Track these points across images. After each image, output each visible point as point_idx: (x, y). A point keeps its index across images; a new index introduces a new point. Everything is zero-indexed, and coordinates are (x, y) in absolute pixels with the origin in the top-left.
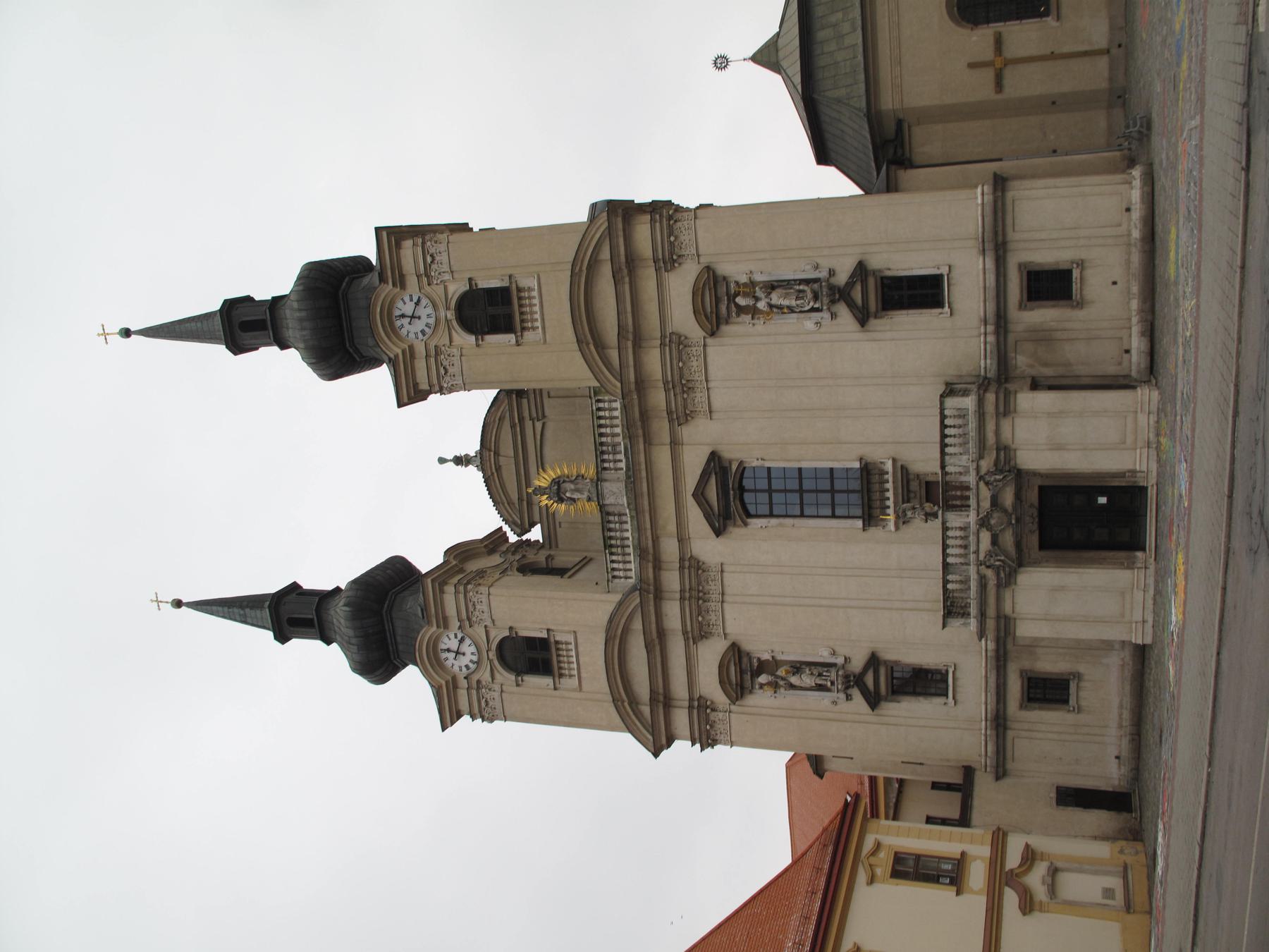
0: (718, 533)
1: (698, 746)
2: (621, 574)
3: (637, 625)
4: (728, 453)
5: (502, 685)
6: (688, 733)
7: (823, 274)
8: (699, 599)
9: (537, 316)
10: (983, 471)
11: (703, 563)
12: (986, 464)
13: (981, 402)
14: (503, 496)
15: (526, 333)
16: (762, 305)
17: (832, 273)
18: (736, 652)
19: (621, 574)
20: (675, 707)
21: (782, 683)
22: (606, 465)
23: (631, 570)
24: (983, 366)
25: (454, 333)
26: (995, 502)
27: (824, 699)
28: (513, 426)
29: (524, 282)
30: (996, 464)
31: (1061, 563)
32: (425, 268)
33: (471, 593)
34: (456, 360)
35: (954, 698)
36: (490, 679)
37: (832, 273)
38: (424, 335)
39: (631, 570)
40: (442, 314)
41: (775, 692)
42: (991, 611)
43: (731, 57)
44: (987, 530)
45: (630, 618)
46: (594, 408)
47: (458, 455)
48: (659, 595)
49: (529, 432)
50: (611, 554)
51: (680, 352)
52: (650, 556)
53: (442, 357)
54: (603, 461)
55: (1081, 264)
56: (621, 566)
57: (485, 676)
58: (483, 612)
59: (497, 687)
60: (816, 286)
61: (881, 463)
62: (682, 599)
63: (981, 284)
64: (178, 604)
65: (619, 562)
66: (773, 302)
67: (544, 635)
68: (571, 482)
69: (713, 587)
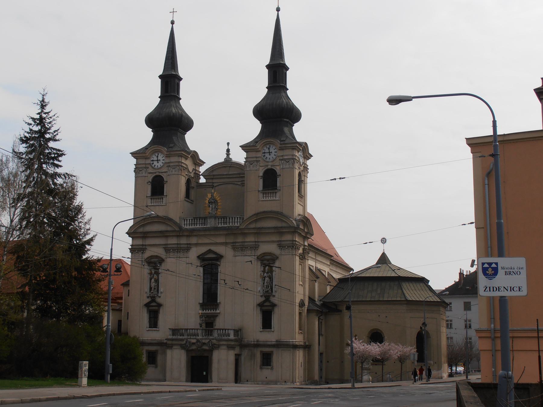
0: (198, 257)
1: (130, 247)
2: (186, 223)
3: (169, 229)
4: (222, 260)
5: (147, 176)
6: (134, 244)
7: (274, 294)
8: (178, 250)
9: (267, 199)
10: (213, 341)
11: (189, 251)
12: (214, 341)
13: (231, 340)
14: (215, 168)
15: (262, 194)
16: (265, 274)
17: (274, 296)
18: (161, 261)
19: (186, 223)
20: (143, 240)
21: (152, 276)
22: (220, 219)
23: (187, 226)
24: (245, 340)
25: (264, 167)
26: (204, 344)
27: (147, 289)
28: (239, 174)
29: (278, 194)
30: (214, 344)
31: (187, 362)
32: (285, 159)
33: (178, 168)
34: (255, 168)
35: (149, 330)
36: (149, 172)
37: (274, 296)
38: (264, 156)
39: (187, 226)
40: (270, 164)
41: (149, 274)
42: (174, 342)
43: (385, 245)
44: (196, 342)
45: (170, 226)
46: (238, 216)
47: (230, 151)
48: (178, 236)
49: (237, 180)
50: (192, 220)
51: (253, 247)
52: (191, 233)
53: (256, 163)
54: (221, 219)
55: (272, 369)
56: (188, 223)
57: (150, 170)
58: (172, 172)
59: (146, 175)
60: (270, 291)
61: (219, 309)
62: (178, 244)
63: (268, 340)
64: (173, 23)
65: (189, 222)
66: (266, 278)
67: (165, 194)
68: (215, 206)
69: (181, 254)
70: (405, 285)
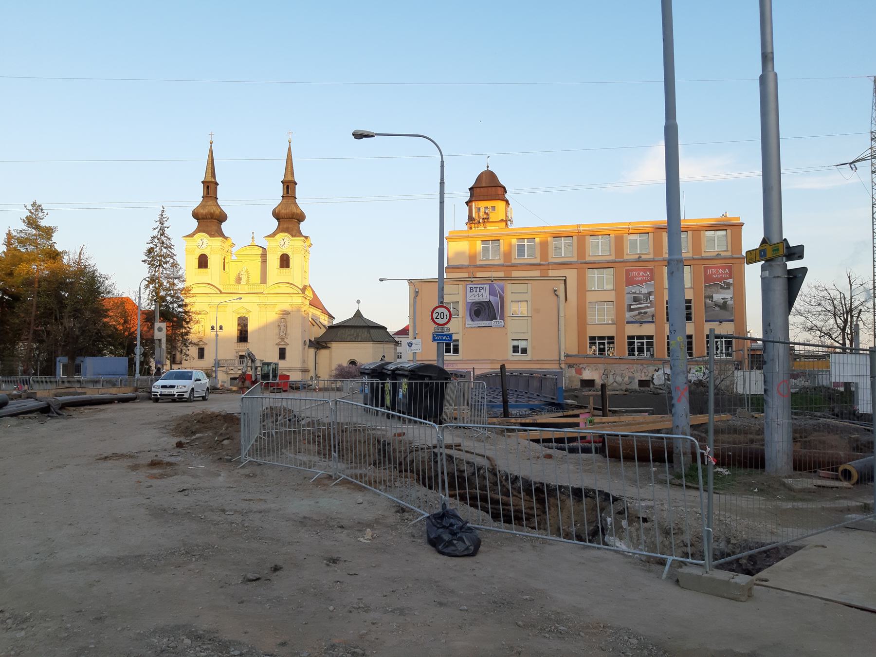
70: (372, 331)
